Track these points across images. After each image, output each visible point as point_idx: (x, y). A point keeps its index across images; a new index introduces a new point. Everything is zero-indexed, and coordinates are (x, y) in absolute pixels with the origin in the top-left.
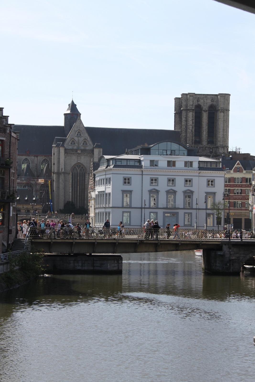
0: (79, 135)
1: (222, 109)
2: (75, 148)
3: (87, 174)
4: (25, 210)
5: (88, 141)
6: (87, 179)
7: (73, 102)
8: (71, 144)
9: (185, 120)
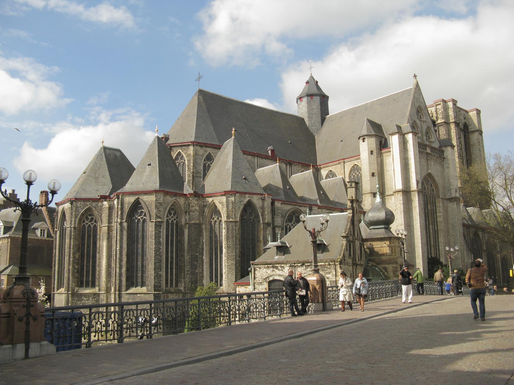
3: (441, 200)
7: (312, 77)
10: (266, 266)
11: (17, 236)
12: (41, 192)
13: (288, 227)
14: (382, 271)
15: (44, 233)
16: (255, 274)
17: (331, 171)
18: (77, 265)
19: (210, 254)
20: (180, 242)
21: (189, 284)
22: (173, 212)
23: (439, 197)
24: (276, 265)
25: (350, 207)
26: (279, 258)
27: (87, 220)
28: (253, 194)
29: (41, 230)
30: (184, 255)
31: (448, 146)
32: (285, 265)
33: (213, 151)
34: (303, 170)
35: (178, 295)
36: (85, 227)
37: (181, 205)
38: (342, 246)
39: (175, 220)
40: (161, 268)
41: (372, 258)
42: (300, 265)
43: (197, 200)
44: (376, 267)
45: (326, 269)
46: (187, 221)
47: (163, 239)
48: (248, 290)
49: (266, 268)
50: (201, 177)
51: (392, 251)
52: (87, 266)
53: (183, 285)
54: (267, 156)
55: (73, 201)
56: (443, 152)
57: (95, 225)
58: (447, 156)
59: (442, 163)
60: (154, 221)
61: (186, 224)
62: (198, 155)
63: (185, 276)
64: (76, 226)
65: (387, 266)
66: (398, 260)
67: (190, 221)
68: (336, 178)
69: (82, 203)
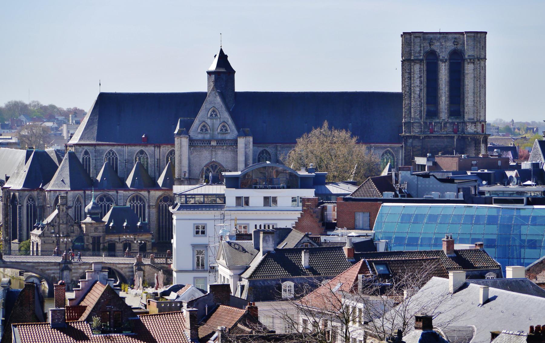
0: (214, 115)
1: (471, 57)
2: (207, 137)
4: (123, 243)
5: (228, 125)
8: (201, 131)
9: (408, 77)
22: (31, 200)
33: (89, 148)
66: (89, 234)
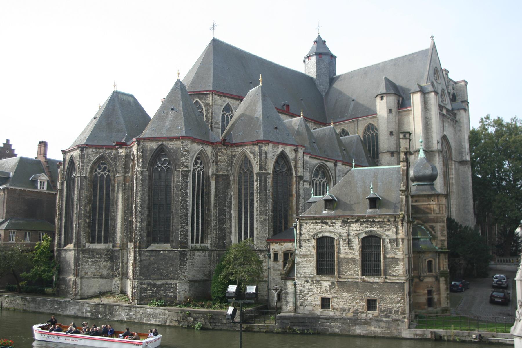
3: (453, 162)
6: (453, 173)
10: (314, 221)
11: (14, 188)
12: (40, 143)
13: (315, 182)
14: (428, 230)
15: (43, 185)
16: (300, 230)
17: (343, 130)
18: (88, 219)
19: (239, 208)
20: (206, 194)
21: (216, 241)
22: (199, 161)
23: (451, 159)
24: (325, 220)
25: (405, 160)
26: (328, 213)
27: (99, 169)
28: (287, 144)
29: (41, 182)
30: (211, 209)
31: (461, 109)
32: (336, 221)
34: (316, 127)
35: (204, 252)
36: (98, 177)
37: (208, 154)
38: (402, 201)
39: (201, 170)
40: (187, 223)
41: (418, 216)
42: (354, 220)
43: (226, 150)
44: (422, 225)
45: (384, 226)
46: (215, 172)
47: (190, 191)
48: (284, 247)
49: (314, 224)
50: (220, 128)
51: (439, 209)
52: (99, 220)
53: (209, 241)
54: (283, 111)
55: (84, 148)
56: (455, 114)
57: (108, 174)
58: (460, 119)
59: (455, 126)
60: (181, 170)
61: (213, 175)
62: (217, 105)
63: (211, 232)
64: (87, 175)
65: (434, 224)
67: (218, 172)
68: (348, 136)
69: (94, 150)
